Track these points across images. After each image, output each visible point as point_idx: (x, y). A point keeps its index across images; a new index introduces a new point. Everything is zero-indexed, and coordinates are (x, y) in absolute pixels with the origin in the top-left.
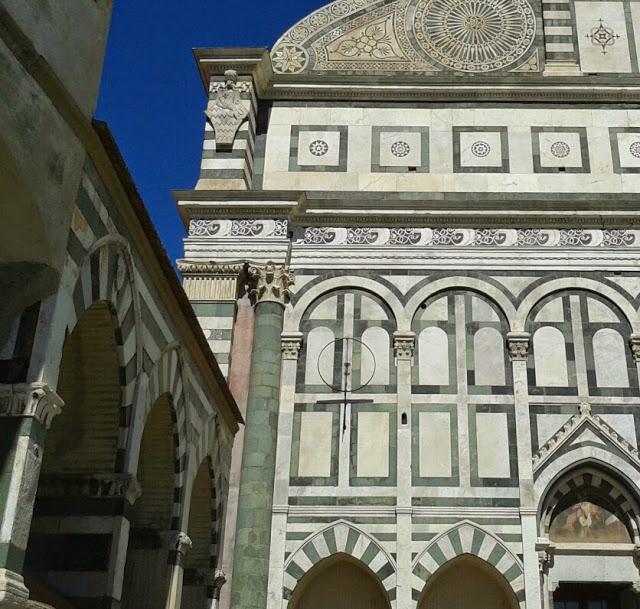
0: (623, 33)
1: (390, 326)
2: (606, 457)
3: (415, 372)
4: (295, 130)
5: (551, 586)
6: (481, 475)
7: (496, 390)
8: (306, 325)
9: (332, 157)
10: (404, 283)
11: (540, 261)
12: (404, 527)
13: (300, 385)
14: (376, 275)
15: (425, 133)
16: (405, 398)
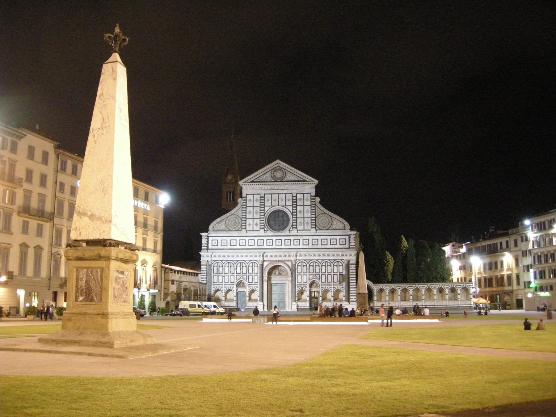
0: (252, 224)
1: (222, 266)
2: (243, 280)
3: (225, 272)
4: (212, 240)
5: (237, 291)
6: (231, 282)
7: (233, 273)
8: (214, 266)
9: (216, 244)
10: (224, 262)
11: (238, 259)
12: (223, 287)
13: (214, 273)
14: (221, 261)
15: (227, 240)
16: (224, 274)
